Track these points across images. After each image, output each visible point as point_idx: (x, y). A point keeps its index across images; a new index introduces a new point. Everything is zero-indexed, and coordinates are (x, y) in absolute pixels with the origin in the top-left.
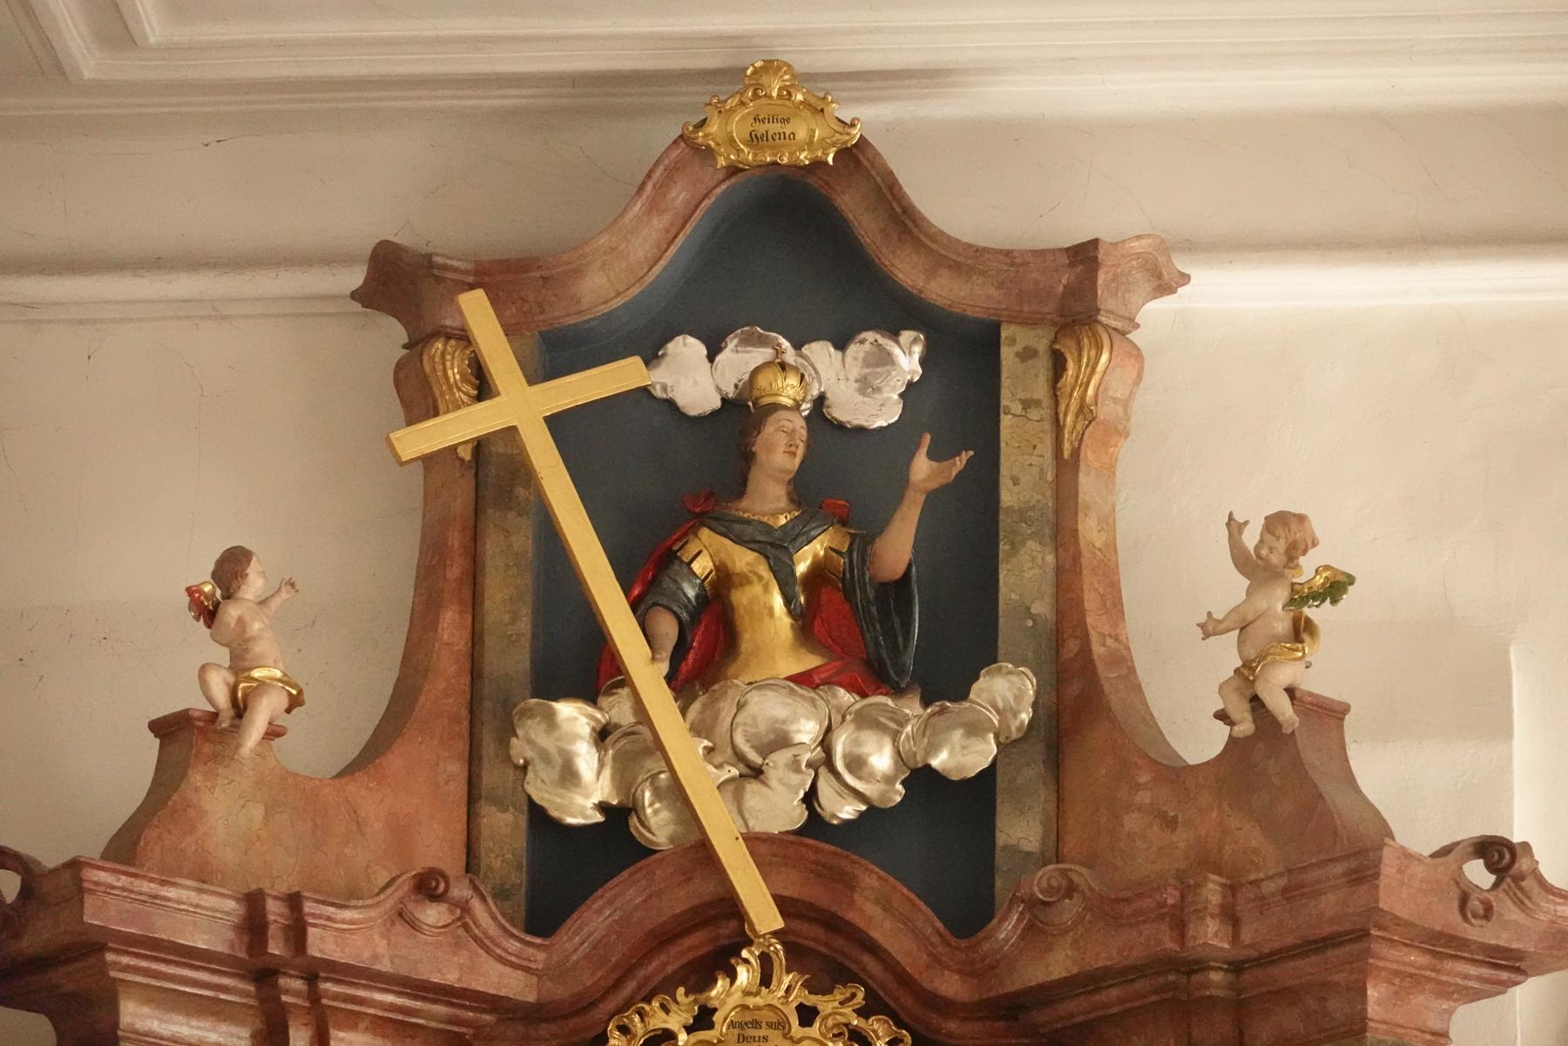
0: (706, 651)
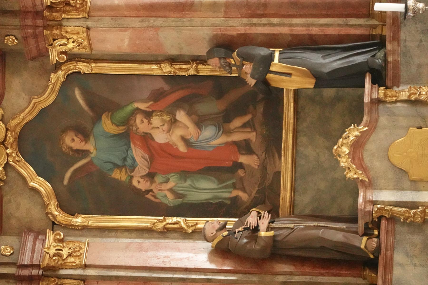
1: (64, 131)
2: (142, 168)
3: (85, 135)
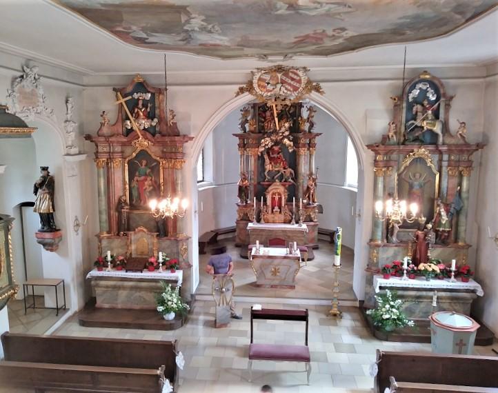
0: (137, 117)
2: (139, 179)
3: (146, 165)
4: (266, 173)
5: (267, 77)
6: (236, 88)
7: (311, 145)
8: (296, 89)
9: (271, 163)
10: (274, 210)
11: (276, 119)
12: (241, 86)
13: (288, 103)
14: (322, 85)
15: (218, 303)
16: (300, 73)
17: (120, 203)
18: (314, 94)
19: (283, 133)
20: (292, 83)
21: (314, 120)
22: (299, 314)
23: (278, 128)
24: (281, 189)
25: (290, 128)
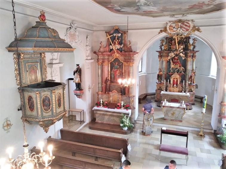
0: (115, 44)
1: (118, 62)
3: (117, 65)
4: (171, 69)
5: (174, 25)
6: (159, 30)
7: (193, 56)
8: (187, 30)
9: (173, 64)
10: (174, 86)
11: (177, 44)
12: (161, 29)
13: (183, 36)
14: (200, 28)
15: (146, 125)
16: (190, 23)
17: (107, 80)
18: (196, 32)
19: (180, 50)
20: (186, 27)
21: (196, 44)
22: (174, 132)
23: (178, 48)
24: (178, 76)
25: (184, 48)
